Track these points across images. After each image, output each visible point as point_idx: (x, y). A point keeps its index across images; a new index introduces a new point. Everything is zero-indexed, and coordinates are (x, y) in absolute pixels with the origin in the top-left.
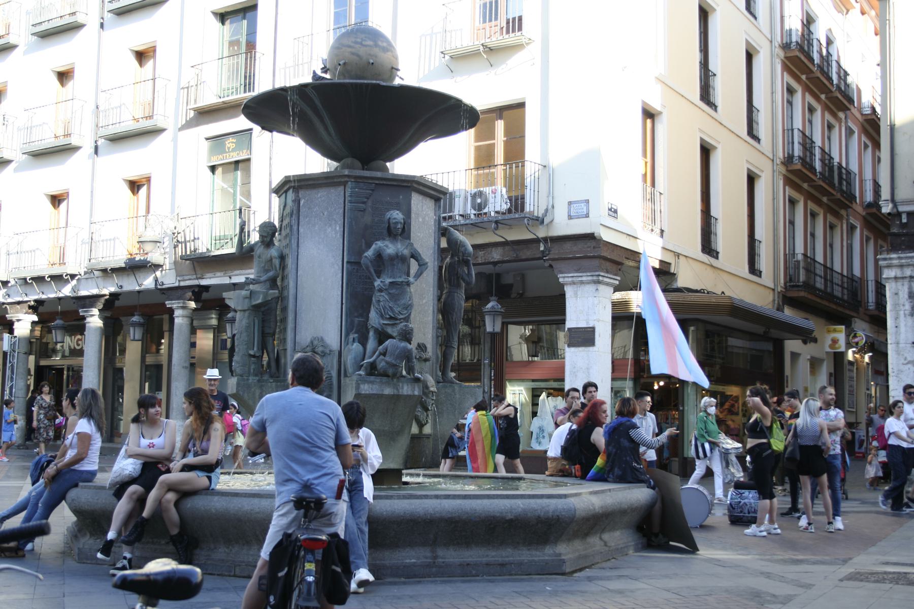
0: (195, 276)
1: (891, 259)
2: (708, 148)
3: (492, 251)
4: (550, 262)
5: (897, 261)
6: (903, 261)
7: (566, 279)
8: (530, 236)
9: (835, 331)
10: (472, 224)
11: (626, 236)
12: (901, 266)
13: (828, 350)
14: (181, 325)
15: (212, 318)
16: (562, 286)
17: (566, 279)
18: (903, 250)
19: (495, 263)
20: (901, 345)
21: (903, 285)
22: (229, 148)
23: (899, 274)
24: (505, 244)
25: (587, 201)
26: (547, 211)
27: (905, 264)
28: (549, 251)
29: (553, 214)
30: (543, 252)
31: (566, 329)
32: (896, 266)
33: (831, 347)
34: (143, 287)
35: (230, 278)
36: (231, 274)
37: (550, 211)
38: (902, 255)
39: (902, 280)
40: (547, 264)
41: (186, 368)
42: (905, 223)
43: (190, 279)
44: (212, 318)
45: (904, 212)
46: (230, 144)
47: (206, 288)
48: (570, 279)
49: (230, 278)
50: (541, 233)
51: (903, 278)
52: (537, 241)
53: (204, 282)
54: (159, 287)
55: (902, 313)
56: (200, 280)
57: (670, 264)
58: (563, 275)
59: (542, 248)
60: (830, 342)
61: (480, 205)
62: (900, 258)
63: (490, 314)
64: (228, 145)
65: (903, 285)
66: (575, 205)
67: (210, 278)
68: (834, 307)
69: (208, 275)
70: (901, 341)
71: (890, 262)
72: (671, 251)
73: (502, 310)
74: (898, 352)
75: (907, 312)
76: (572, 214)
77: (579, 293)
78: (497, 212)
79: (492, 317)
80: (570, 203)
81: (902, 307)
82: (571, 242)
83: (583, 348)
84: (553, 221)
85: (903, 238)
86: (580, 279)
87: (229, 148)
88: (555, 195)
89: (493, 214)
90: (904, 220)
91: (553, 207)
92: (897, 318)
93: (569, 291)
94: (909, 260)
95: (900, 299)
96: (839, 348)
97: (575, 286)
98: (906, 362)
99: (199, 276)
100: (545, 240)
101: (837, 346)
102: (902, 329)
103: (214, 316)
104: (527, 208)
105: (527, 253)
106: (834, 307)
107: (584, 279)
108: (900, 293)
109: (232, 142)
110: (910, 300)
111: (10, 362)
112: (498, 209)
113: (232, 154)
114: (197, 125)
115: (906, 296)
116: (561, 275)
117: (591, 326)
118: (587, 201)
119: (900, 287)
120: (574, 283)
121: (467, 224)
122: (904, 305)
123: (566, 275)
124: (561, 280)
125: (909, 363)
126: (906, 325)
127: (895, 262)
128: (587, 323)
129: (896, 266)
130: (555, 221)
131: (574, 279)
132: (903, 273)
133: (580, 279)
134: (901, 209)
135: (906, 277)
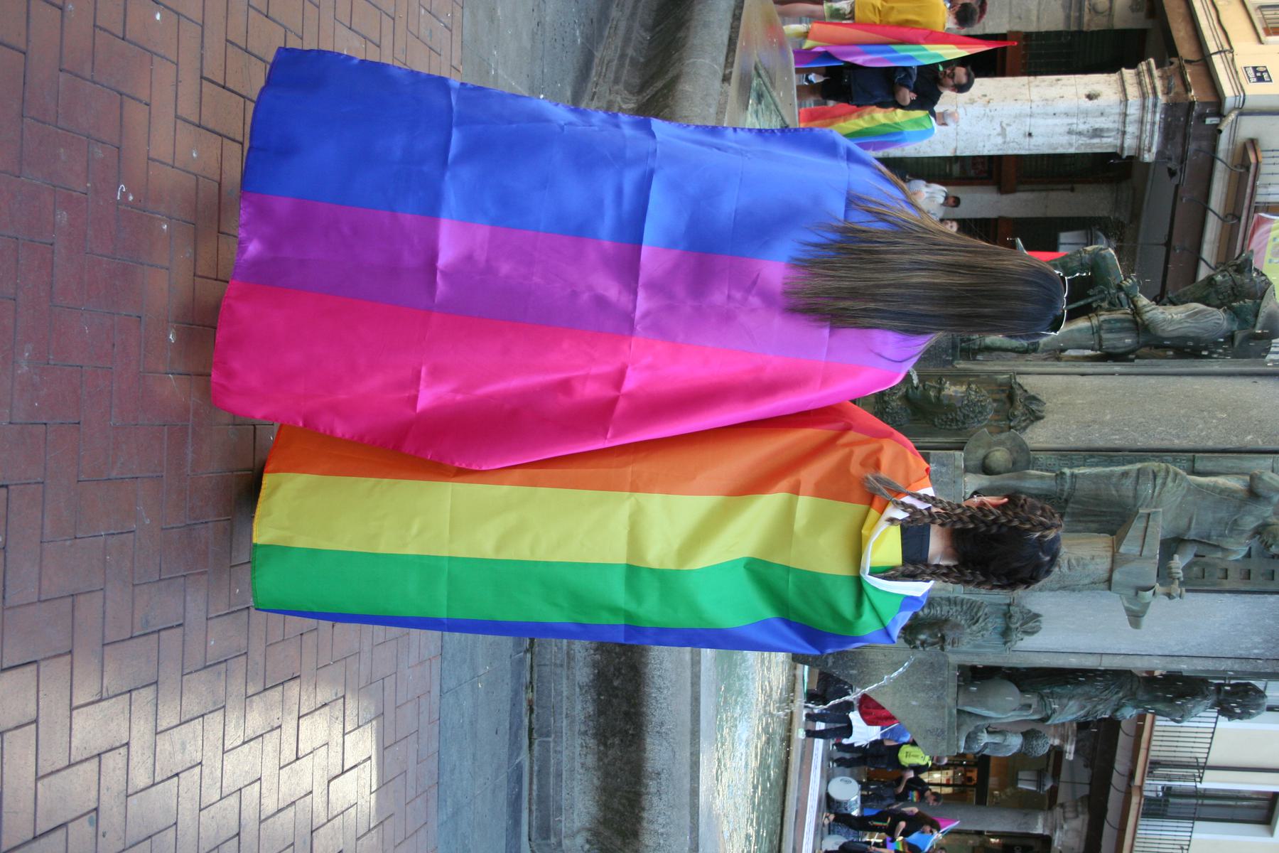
1: (1154, 112)
6: (1148, 127)
12: (1141, 122)
20: (1028, 119)
21: (1114, 122)
27: (1144, 128)
32: (1143, 117)
38: (1157, 127)
39: (1121, 120)
51: (1124, 123)
55: (1075, 120)
62: (1153, 123)
65: (1114, 122)
70: (1033, 120)
71: (1150, 111)
75: (1074, 127)
81: (1082, 120)
94: (1148, 134)
98: (1004, 125)
102: (1051, 121)
108: (1103, 119)
115: (1097, 126)
119: (1111, 118)
122: (1085, 123)
125: (1002, 127)
126: (1056, 125)
127: (1149, 117)
129: (1143, 117)
132: (1131, 123)
135: (1125, 127)
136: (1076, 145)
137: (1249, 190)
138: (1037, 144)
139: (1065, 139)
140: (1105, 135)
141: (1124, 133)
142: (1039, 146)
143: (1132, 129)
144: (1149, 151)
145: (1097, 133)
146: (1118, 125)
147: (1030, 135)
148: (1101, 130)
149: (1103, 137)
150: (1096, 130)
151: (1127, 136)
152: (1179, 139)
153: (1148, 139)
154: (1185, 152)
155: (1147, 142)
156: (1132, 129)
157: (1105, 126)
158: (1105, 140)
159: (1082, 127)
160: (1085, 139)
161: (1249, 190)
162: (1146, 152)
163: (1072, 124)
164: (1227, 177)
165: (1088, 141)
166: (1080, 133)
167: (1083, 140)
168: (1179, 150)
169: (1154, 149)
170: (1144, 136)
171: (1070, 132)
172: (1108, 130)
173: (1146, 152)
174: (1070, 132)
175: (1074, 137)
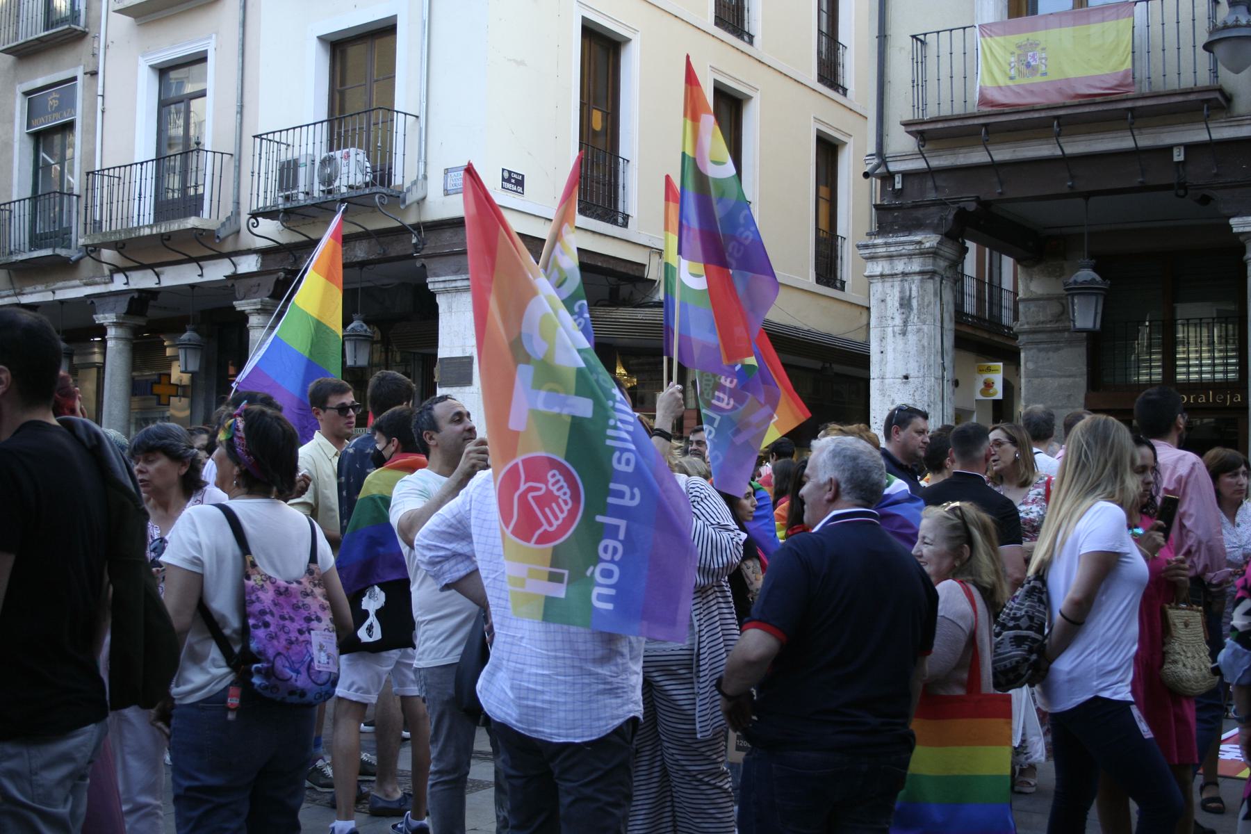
0: (12, 292)
1: (874, 246)
2: (740, 97)
3: (355, 246)
5: (884, 249)
9: (989, 370)
10: (313, 205)
11: (543, 221)
12: (890, 257)
13: (980, 397)
15: (94, 353)
16: (433, 296)
18: (895, 232)
20: (887, 381)
22: (51, 107)
23: (887, 272)
25: (503, 170)
26: (415, 183)
27: (895, 253)
28: (424, 244)
32: (882, 257)
33: (983, 392)
35: (54, 293)
36: (53, 287)
37: (419, 184)
38: (890, 240)
39: (891, 280)
40: (418, 264)
42: (899, 189)
43: (8, 296)
44: (94, 353)
45: (898, 172)
46: (54, 101)
48: (442, 285)
49: (54, 293)
50: (411, 219)
51: (892, 275)
52: (403, 230)
56: (20, 297)
57: (643, 266)
59: (414, 241)
60: (982, 386)
61: (330, 176)
62: (887, 244)
63: (350, 340)
66: (453, 174)
67: (32, 293)
68: (986, 335)
69: (28, 289)
71: (873, 250)
72: (645, 246)
74: (883, 393)
75: (897, 329)
76: (449, 188)
77: (454, 305)
78: (351, 187)
79: (353, 342)
80: (447, 171)
81: (890, 322)
82: (451, 230)
83: (458, 388)
84: (424, 199)
85: (896, 214)
86: (454, 284)
87: (51, 107)
88: (429, 160)
89: (344, 190)
90: (898, 186)
91: (425, 177)
92: (882, 339)
93: (441, 301)
94: (901, 248)
95: (889, 309)
96: (995, 393)
97: (449, 295)
99: (17, 291)
100: (417, 227)
101: (991, 391)
102: (890, 355)
103: (96, 350)
104: (397, 180)
105: (396, 249)
106: (986, 335)
107: (459, 284)
108: (888, 299)
109: (55, 98)
110: (903, 310)
112: (351, 182)
113: (54, 115)
115: (897, 304)
117: (468, 355)
118: (503, 170)
120: (447, 291)
121: (306, 206)
124: (430, 287)
127: (881, 250)
128: (464, 350)
129: (882, 257)
130: (429, 198)
131: (447, 285)
132: (893, 268)
133: (454, 284)
134: (893, 167)
135: (896, 274)
136: (919, 325)
137: (940, 125)
138: (917, 369)
139: (912, 338)
140: (908, 294)
141: (904, 274)
142: (920, 366)
143: (900, 266)
144: (920, 243)
145: (905, 303)
146: (897, 284)
147: (906, 377)
148: (902, 299)
149: (910, 296)
150: (901, 305)
151: (907, 271)
152: (919, 213)
153: (907, 247)
154: (934, 203)
155: (911, 247)
156: (900, 266)
157: (897, 295)
158: (914, 293)
159: (898, 321)
160: (912, 317)
161: (940, 125)
162: (923, 246)
163: (894, 332)
164: (962, 151)
165: (915, 311)
166: (905, 323)
167: (914, 317)
168: (933, 209)
169: (918, 238)
170: (904, 251)
171: (904, 333)
172: (902, 291)
173: (923, 246)
174: (904, 333)
175: (909, 328)
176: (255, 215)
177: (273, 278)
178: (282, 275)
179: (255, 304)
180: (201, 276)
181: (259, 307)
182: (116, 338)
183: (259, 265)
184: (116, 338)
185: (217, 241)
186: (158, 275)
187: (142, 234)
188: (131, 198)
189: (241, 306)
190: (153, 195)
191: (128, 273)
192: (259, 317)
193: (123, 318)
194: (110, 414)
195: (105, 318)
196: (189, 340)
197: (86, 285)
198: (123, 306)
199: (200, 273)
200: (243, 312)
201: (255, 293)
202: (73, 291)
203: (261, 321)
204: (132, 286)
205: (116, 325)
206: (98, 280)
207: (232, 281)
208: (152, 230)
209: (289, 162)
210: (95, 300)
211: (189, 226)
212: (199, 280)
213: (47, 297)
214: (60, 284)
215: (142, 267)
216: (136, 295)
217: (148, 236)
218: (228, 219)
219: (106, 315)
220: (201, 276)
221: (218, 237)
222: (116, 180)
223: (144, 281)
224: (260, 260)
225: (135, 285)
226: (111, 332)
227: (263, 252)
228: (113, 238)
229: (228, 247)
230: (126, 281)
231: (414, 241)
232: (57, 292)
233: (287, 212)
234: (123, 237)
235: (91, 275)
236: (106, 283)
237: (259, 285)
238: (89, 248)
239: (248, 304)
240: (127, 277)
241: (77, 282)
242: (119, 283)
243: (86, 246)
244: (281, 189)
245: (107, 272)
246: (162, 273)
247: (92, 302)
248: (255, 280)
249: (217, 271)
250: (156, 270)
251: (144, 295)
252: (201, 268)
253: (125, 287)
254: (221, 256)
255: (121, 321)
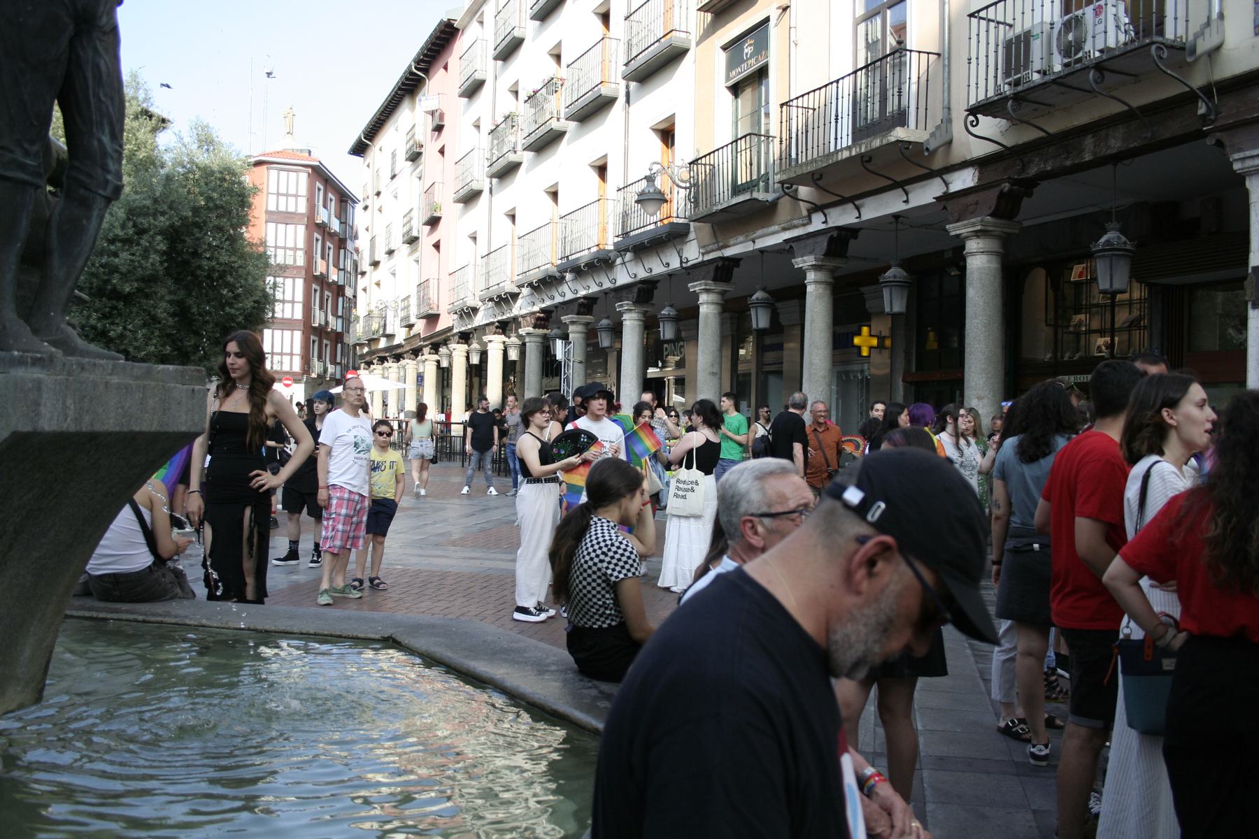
4: (1218, 135)
7: (1249, 163)
8: (1174, 90)
14: (707, 316)
17: (1249, 163)
19: (1116, 158)
24: (1130, 116)
28: (1217, 113)
29: (1221, 31)
30: (1203, 116)
31: (1250, 271)
34: (670, 268)
35: (754, 242)
36: (754, 236)
37: (1214, 25)
41: (714, 374)
46: (749, 48)
47: (735, 261)
49: (754, 242)
52: (1190, 98)
53: (728, 252)
54: (684, 265)
56: (723, 251)
58: (1241, 155)
59: (1202, 110)
63: (1103, 256)
64: (746, 51)
69: (732, 242)
73: (1128, 247)
84: (1218, 48)
91: (1221, 16)
99: (721, 244)
100: (1207, 90)
104: (1169, 34)
111: (565, 374)
114: (714, 32)
116: (1236, 156)
123: (1248, 153)
124: (1237, 166)
130: (1224, 50)
176: (974, 111)
177: (993, 194)
178: (1006, 186)
179: (974, 225)
180: (906, 202)
181: (979, 228)
182: (816, 282)
183: (976, 180)
184: (816, 282)
185: (926, 154)
186: (858, 208)
187: (839, 158)
188: (827, 123)
189: (955, 229)
190: (851, 113)
191: (826, 211)
192: (978, 241)
193: (822, 260)
194: (811, 364)
195: (804, 261)
196: (895, 276)
197: (785, 229)
198: (823, 243)
199: (905, 199)
200: (958, 236)
201: (972, 213)
202: (772, 238)
203: (981, 245)
204: (831, 224)
205: (816, 268)
206: (795, 222)
207: (943, 203)
208: (850, 152)
209: (1018, 38)
210: (793, 245)
211: (892, 139)
212: (904, 207)
213: (748, 247)
214: (759, 232)
215: (843, 201)
216: (835, 234)
217: (847, 159)
218: (938, 127)
219: (805, 258)
220: (906, 202)
221: (927, 149)
222: (811, 111)
223: (844, 217)
224: (977, 174)
225: (834, 223)
226: (811, 276)
227: (981, 163)
228: (809, 169)
229: (938, 164)
230: (824, 220)
231: (1202, 110)
232: (756, 241)
233: (1017, 97)
234: (821, 165)
235: (789, 218)
236: (804, 225)
237: (977, 203)
238: (786, 186)
239: (965, 226)
240: (825, 215)
241: (776, 228)
242: (817, 223)
243: (782, 183)
244: (1007, 74)
245: (805, 213)
246: (862, 205)
247: (791, 247)
248: (971, 199)
249: (926, 194)
250: (857, 203)
251: (843, 233)
252: (907, 194)
253: (823, 226)
254: (931, 175)
255: (820, 263)
